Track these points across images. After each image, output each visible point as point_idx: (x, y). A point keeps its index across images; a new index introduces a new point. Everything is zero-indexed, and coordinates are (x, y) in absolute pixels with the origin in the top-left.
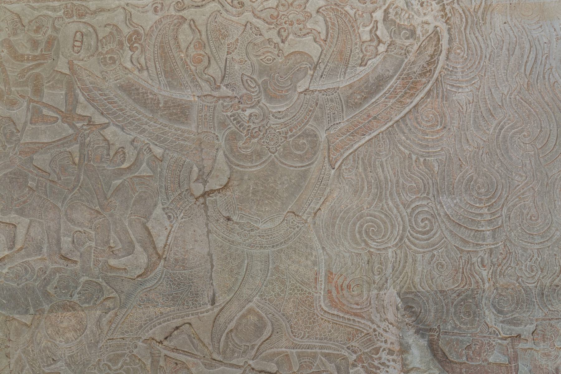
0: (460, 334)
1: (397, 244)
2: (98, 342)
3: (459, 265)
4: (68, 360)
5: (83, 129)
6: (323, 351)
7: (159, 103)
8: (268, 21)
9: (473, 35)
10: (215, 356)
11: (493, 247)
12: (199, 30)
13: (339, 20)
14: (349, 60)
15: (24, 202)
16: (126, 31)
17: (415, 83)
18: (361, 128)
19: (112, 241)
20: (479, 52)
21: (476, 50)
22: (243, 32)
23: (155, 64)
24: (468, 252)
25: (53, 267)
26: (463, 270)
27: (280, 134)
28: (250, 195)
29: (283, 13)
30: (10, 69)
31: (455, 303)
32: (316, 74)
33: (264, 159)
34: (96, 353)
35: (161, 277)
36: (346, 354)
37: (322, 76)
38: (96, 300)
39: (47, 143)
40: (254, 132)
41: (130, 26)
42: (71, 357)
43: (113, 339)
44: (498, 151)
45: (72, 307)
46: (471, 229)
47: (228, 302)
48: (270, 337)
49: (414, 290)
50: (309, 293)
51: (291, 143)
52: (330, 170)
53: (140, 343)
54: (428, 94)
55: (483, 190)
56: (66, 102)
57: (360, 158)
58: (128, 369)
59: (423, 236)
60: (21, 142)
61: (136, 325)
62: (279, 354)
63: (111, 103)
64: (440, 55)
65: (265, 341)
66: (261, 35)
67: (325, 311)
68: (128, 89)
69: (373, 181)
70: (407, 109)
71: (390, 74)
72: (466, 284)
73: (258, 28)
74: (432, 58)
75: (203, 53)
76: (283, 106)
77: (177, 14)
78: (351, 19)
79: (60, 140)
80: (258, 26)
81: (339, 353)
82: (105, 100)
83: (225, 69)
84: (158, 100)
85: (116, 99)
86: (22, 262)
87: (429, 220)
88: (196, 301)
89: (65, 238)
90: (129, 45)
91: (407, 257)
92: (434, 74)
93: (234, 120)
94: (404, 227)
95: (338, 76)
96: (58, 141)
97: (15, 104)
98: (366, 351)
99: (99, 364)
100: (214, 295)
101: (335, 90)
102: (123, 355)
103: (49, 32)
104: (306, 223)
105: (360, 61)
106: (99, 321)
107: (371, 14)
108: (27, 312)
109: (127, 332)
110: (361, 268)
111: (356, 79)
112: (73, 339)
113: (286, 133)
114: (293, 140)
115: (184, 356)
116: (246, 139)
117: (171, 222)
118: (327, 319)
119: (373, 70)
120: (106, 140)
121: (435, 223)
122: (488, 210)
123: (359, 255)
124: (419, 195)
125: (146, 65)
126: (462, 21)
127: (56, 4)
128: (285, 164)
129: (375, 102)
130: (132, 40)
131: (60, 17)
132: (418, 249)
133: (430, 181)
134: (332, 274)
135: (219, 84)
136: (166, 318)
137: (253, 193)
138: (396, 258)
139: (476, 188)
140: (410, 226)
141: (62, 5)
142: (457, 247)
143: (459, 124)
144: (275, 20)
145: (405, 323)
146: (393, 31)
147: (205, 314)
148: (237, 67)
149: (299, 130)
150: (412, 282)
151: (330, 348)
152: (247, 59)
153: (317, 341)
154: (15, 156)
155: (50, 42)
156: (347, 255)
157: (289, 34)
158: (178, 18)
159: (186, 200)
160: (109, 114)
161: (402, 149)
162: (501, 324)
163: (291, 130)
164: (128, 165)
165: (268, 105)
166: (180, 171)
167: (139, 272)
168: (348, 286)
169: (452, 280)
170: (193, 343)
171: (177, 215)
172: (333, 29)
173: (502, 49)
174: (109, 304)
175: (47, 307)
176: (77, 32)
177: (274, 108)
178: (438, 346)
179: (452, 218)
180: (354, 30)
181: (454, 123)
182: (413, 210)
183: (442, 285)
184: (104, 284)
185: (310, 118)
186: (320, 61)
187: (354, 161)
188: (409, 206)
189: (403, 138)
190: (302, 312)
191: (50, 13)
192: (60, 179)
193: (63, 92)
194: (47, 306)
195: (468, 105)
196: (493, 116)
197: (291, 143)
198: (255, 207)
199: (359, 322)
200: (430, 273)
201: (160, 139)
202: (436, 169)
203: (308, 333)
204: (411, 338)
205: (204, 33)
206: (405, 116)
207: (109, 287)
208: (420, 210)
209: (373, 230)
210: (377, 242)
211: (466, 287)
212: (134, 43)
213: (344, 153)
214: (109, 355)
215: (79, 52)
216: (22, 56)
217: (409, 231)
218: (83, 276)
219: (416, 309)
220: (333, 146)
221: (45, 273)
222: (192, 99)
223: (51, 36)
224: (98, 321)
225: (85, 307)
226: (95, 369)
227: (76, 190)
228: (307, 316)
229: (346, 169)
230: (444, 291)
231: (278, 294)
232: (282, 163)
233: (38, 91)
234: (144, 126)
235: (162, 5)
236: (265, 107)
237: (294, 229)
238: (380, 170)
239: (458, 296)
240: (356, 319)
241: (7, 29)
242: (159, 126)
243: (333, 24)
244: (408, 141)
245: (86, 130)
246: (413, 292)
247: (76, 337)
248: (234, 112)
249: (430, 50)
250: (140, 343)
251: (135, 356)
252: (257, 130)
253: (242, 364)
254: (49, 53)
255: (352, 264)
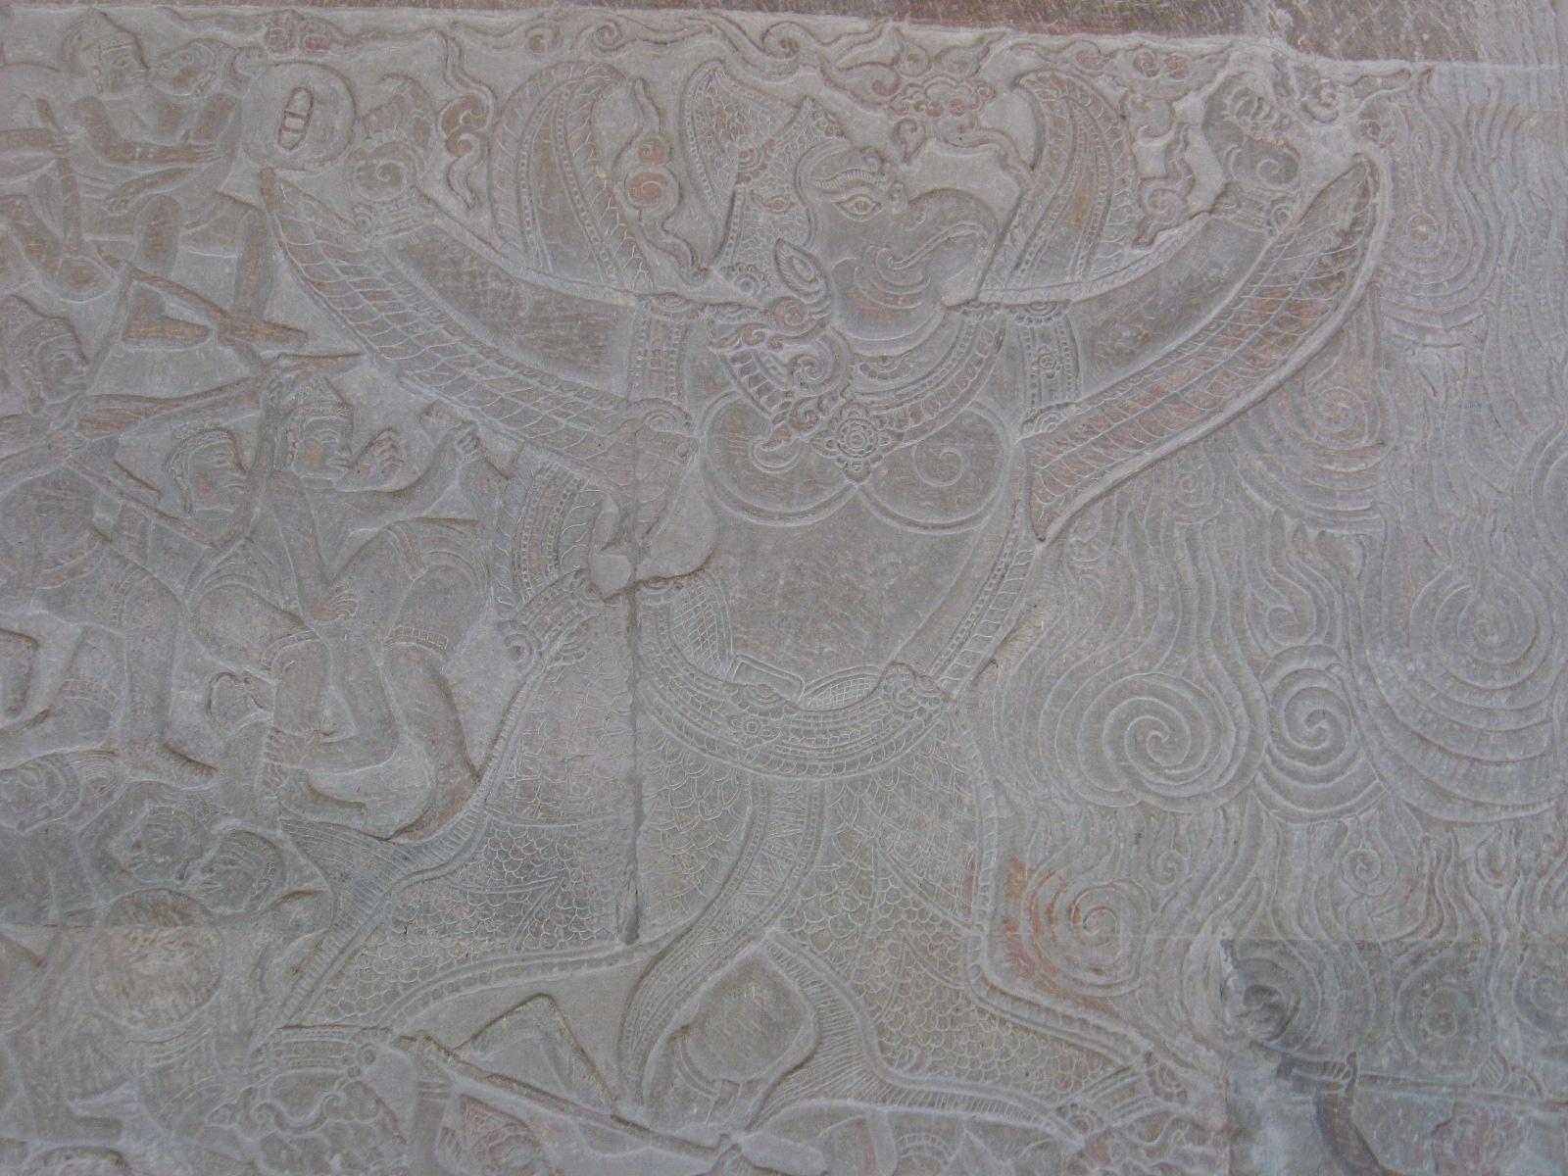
0: (1418, 1085)
1: (1229, 787)
2: (250, 1033)
3: (1421, 864)
4: (149, 1084)
5: (278, 367)
6: (980, 1116)
7: (516, 307)
8: (866, 97)
9: (1462, 188)
10: (626, 1109)
11: (1521, 814)
12: (657, 109)
13: (1076, 111)
14: (1102, 225)
15: (73, 572)
16: (444, 94)
17: (1296, 307)
18: (1130, 425)
19: (327, 712)
20: (1481, 237)
21: (1474, 232)
22: (790, 123)
23: (518, 192)
24: (1449, 826)
25: (137, 779)
26: (1431, 880)
27: (882, 423)
28: (777, 602)
29: (911, 80)
30: (87, 181)
31: (1404, 985)
32: (999, 258)
33: (827, 495)
34: (241, 1069)
35: (471, 840)
36: (1054, 1131)
37: (1017, 266)
38: (258, 897)
39: (165, 401)
40: (801, 410)
41: (458, 86)
42: (163, 1072)
43: (299, 1026)
44: (1540, 525)
45: (175, 911)
46: (1458, 756)
47: (679, 938)
48: (807, 1060)
49: (1278, 936)
50: (945, 925)
51: (913, 454)
52: (1030, 545)
53: (385, 1048)
54: (1334, 340)
55: (1495, 639)
56: (238, 284)
57: (1126, 514)
58: (339, 1127)
59: (1312, 769)
60: (89, 392)
61: (377, 987)
62: (835, 1115)
63: (373, 297)
64: (1369, 234)
65: (790, 1072)
66: (841, 134)
67: (993, 988)
68: (428, 257)
69: (1162, 587)
70: (1271, 380)
71: (1224, 274)
72: (1440, 926)
73: (834, 115)
74: (1346, 241)
75: (665, 173)
76: (895, 344)
77: (598, 59)
78: (1112, 113)
79: (206, 394)
80: (835, 108)
81: (1029, 1125)
82: (355, 284)
83: (728, 222)
84: (517, 297)
85: (390, 286)
86: (45, 758)
87: (1333, 721)
88: (578, 924)
89: (184, 693)
90: (445, 136)
91: (1259, 828)
92: (1351, 286)
93: (743, 371)
94: (1253, 735)
95: (1068, 269)
96: (198, 396)
97: (87, 281)
98: (1119, 1124)
99: (246, 1105)
100: (638, 911)
101: (1057, 306)
102: (328, 1081)
103: (217, 86)
104: (947, 700)
105: (1133, 233)
106: (261, 963)
107: (1170, 104)
108: (37, 915)
109: (346, 1007)
110: (1115, 856)
111: (1119, 283)
112: (174, 1014)
113: (902, 423)
114: (921, 446)
115: (525, 1102)
116: (778, 431)
117: (520, 667)
118: (997, 1013)
119: (1171, 261)
120: (344, 403)
121: (1349, 729)
122: (1511, 700)
123: (1108, 812)
124: (1302, 642)
125: (489, 193)
126: (1431, 146)
127: (249, 10)
128: (894, 517)
129: (1177, 352)
130: (456, 123)
131: (256, 47)
132: (1293, 807)
133: (1338, 601)
134: (1020, 867)
135: (704, 265)
136: (478, 973)
137: (785, 597)
138: (1227, 831)
139: (1476, 630)
140: (1272, 733)
141: (265, 14)
142: (1414, 809)
143: (1425, 436)
144: (888, 98)
145: (1246, 1042)
146: (1232, 158)
147: (604, 969)
148: (763, 218)
149: (944, 415)
150: (1275, 912)
151: (1002, 1108)
152: (794, 199)
153: (962, 1081)
154: (66, 432)
155: (216, 113)
156: (1072, 810)
157: (924, 139)
158: (600, 72)
159: (573, 602)
160: (362, 328)
161: (1256, 497)
162: (1542, 1062)
163: (916, 414)
164: (403, 484)
165: (851, 335)
166: (563, 514)
167: (400, 817)
168: (1069, 911)
169: (1396, 911)
170: (557, 1061)
171: (540, 645)
172: (1059, 136)
173: (1546, 234)
174: (297, 910)
175: (102, 904)
176: (295, 91)
177: (869, 345)
178: (1348, 1121)
179: (1402, 718)
180: (1120, 145)
181: (1411, 433)
182: (1284, 684)
183: (1364, 927)
184: (290, 846)
185: (977, 382)
186: (1015, 223)
187: (1106, 521)
188: (1271, 671)
189: (1259, 464)
190: (918, 986)
191: (226, 35)
192: (191, 511)
193: (234, 256)
194: (101, 902)
195: (1450, 384)
196: (1525, 422)
197: (913, 454)
198: (788, 642)
199: (1098, 1028)
200: (1331, 886)
201: (511, 412)
202: (1355, 565)
203: (935, 1053)
204: (1263, 1088)
205: (671, 118)
206: (1264, 399)
207: (302, 860)
208: (1303, 684)
209: (1156, 737)
210: (1169, 778)
211: (1439, 937)
212: (460, 132)
213: (1076, 494)
214: (284, 1079)
215: (296, 145)
216: (129, 146)
217: (1269, 750)
218: (227, 815)
219: (1282, 997)
220: (1043, 472)
221: (110, 796)
222: (621, 302)
223: (220, 96)
224: (257, 965)
225: (223, 917)
226: (233, 1118)
227: (233, 549)
228: (932, 1000)
229: (1081, 544)
230: (1372, 946)
231: (847, 924)
232: (887, 513)
233: (159, 246)
234: (464, 371)
235: (557, 34)
236: (840, 341)
237: (909, 717)
238: (1183, 554)
239: (1416, 961)
240: (1093, 1019)
241: (96, 72)
242: (511, 373)
243: (1059, 123)
244: (1273, 476)
245: (285, 370)
246: (1274, 944)
247: (183, 1009)
248: (745, 348)
249: (1344, 220)
250: (385, 1048)
251: (367, 1090)
252: (810, 405)
253: (710, 1142)
254: (208, 142)
255: (1087, 841)
